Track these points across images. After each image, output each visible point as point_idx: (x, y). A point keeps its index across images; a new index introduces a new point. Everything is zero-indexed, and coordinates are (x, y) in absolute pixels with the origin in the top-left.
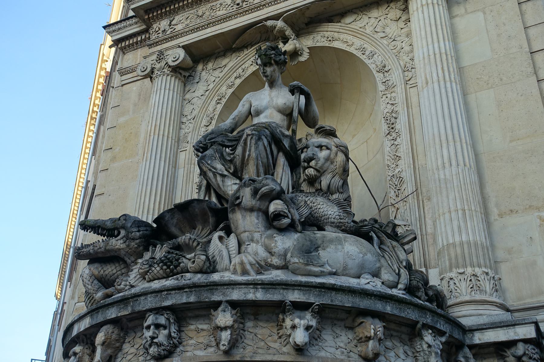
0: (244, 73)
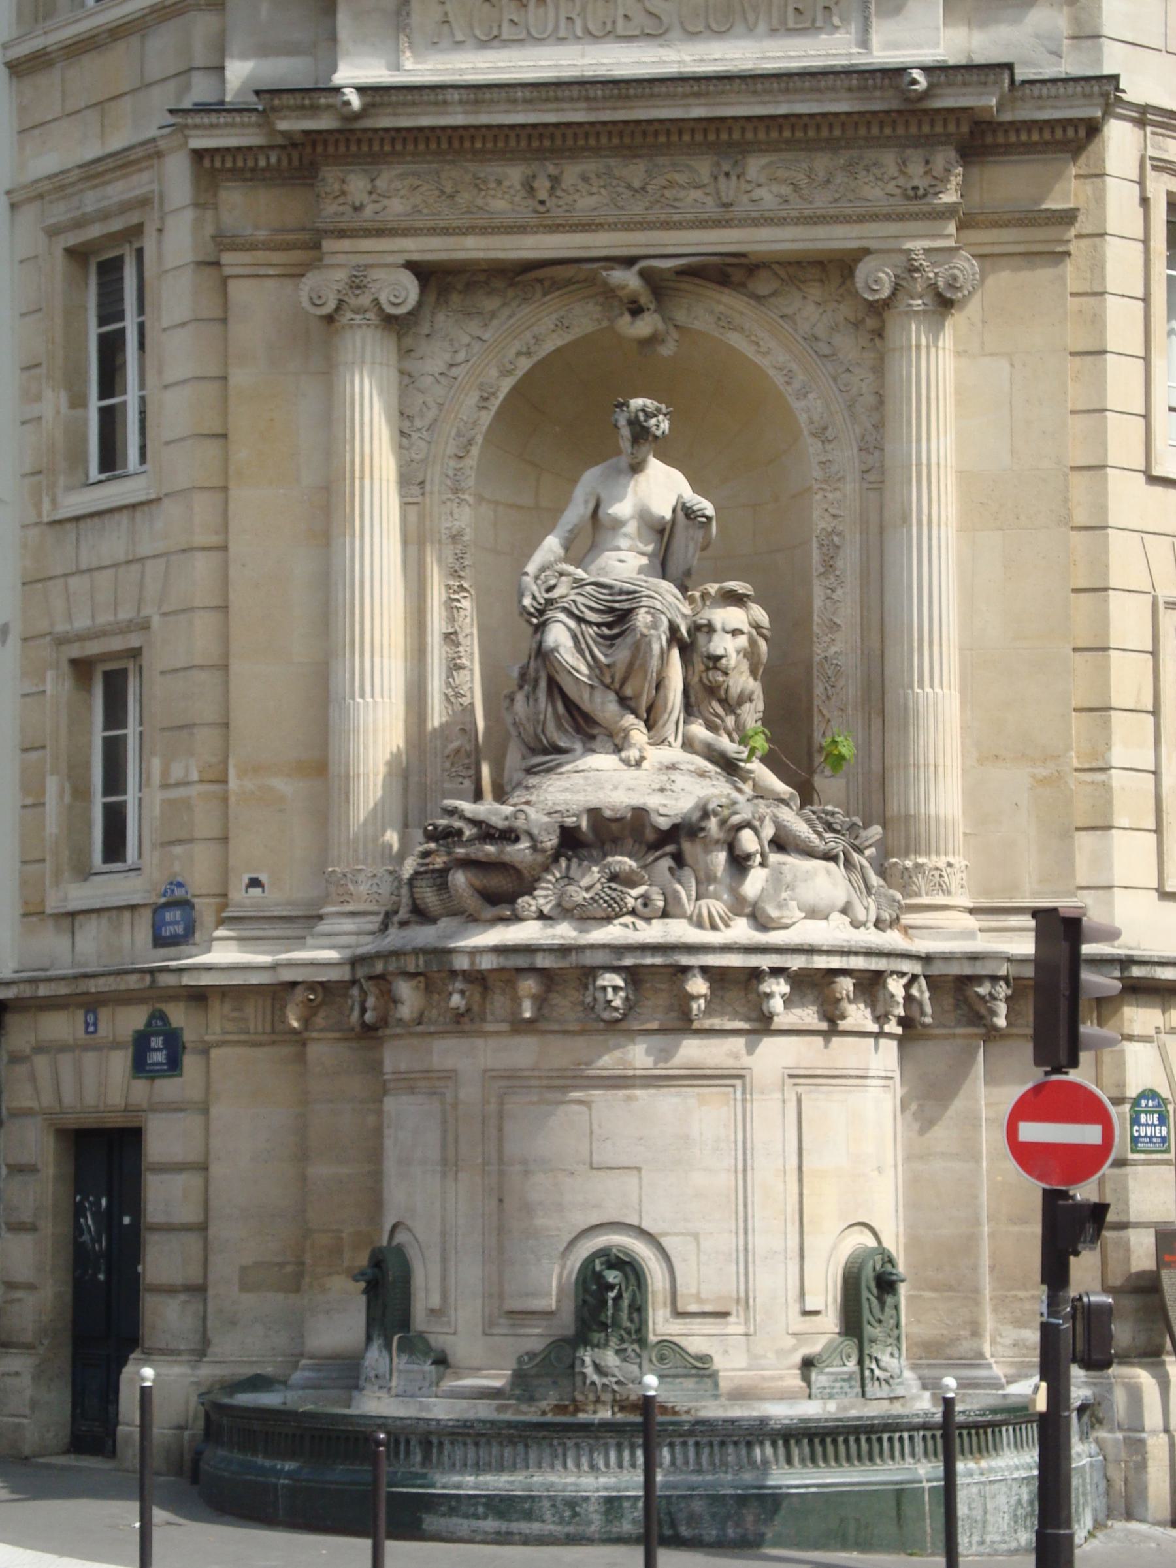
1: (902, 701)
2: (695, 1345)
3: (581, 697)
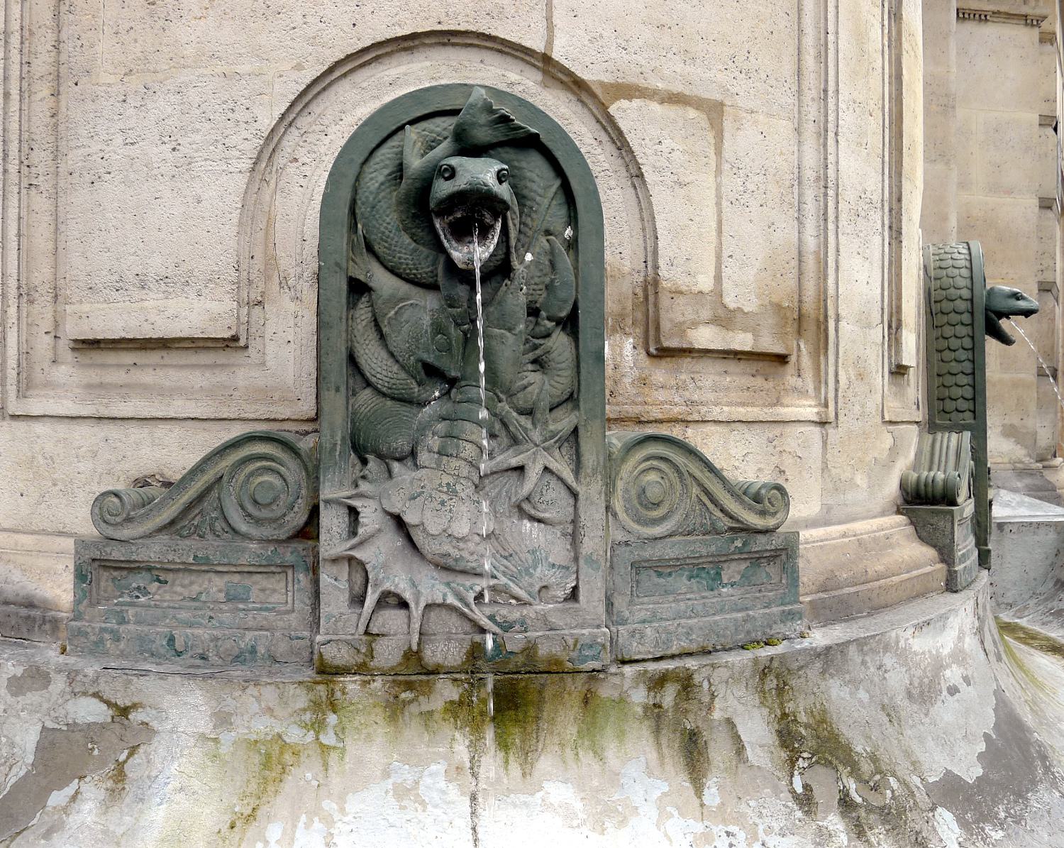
2: (739, 457)
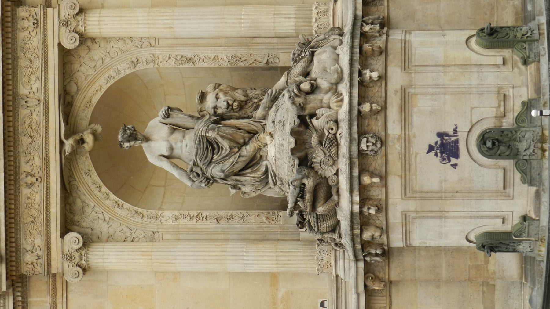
0: (97, 184)
1: (247, 28)
2: (518, 108)
3: (244, 161)
